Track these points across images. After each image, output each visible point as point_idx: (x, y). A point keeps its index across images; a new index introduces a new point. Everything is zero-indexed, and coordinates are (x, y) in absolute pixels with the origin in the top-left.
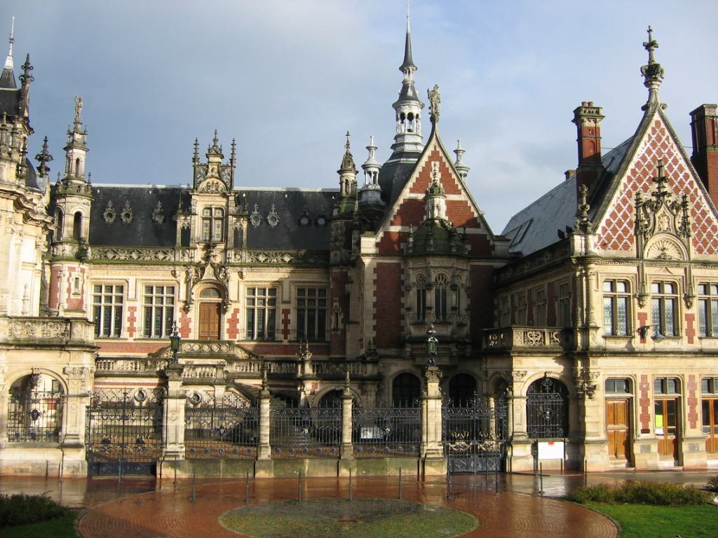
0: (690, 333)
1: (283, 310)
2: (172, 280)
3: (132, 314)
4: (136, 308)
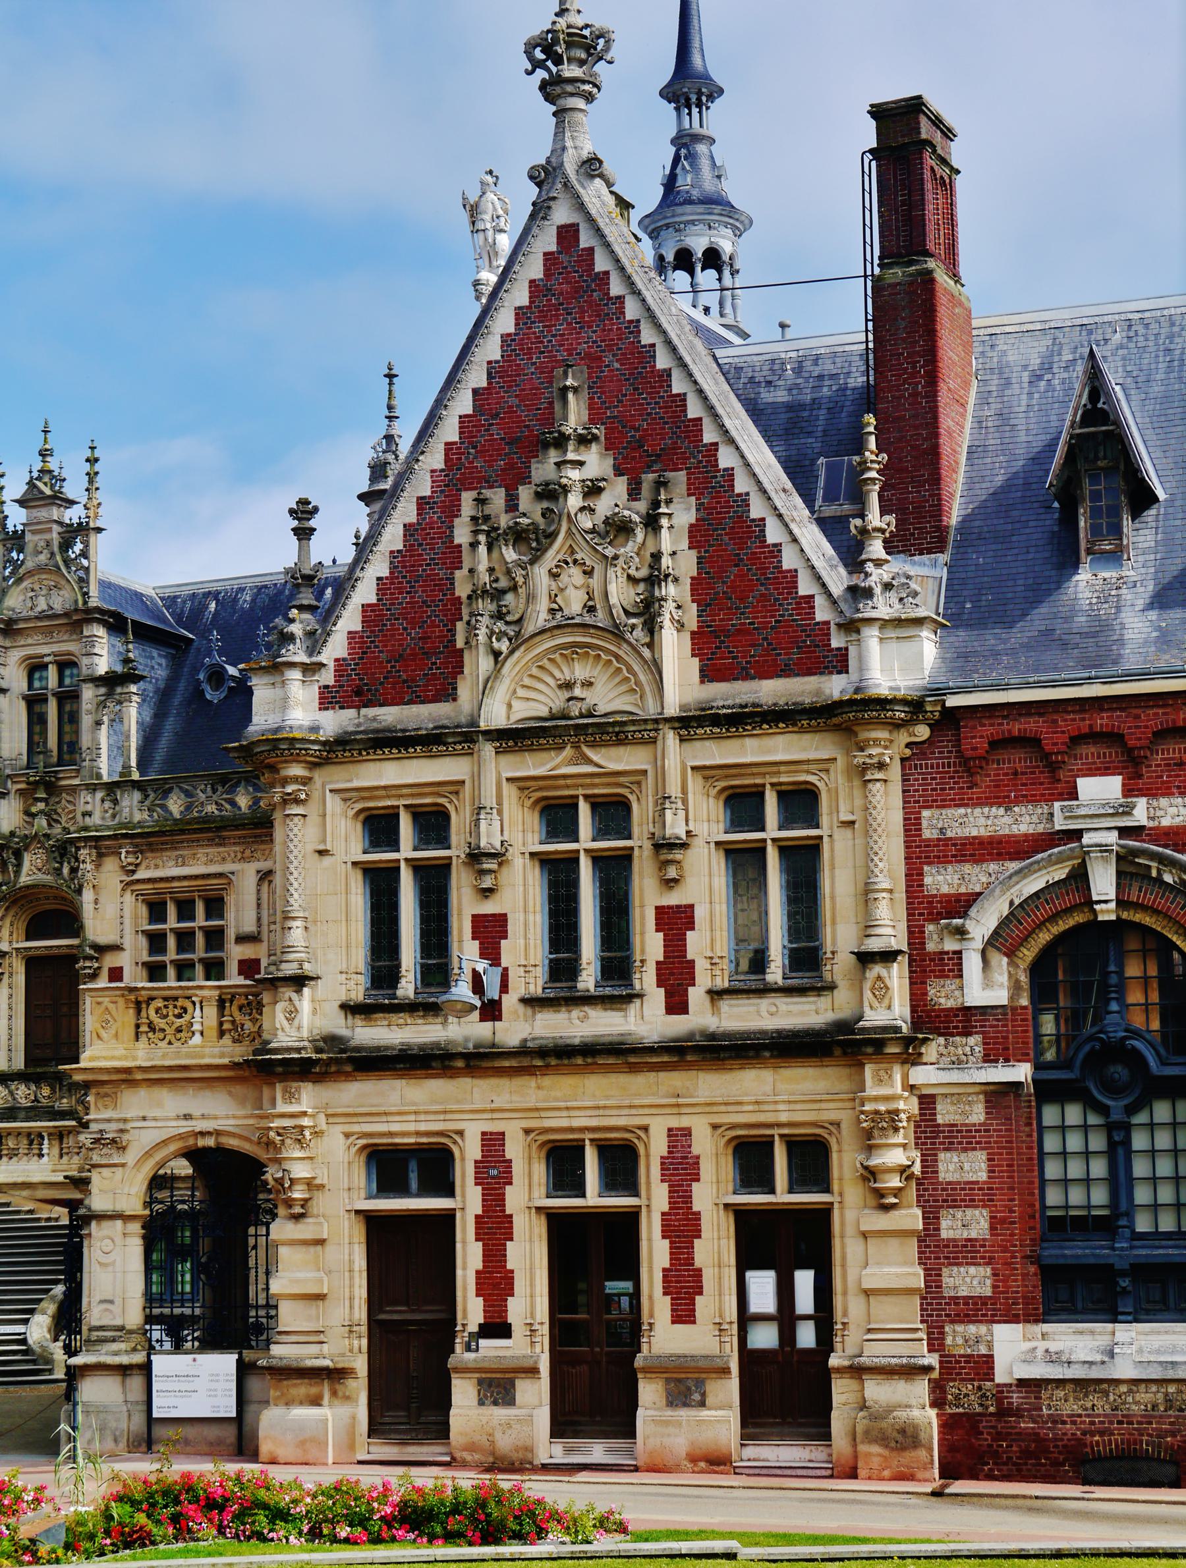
0: (676, 977)
1: (241, 962)
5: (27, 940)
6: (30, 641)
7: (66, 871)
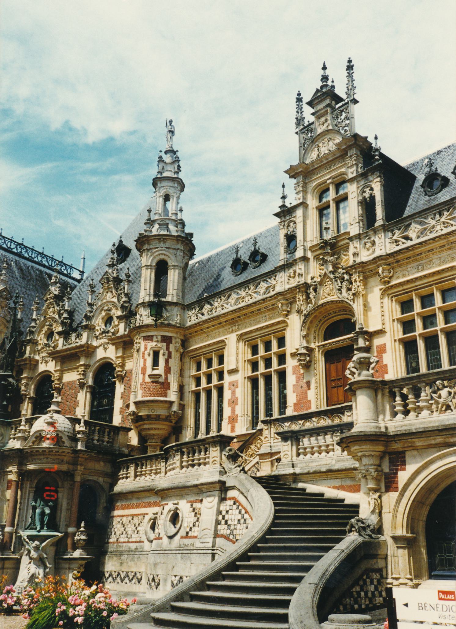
2: (278, 323)
3: (233, 393)
4: (237, 382)
5: (324, 341)
6: (319, 175)
7: (344, 290)
